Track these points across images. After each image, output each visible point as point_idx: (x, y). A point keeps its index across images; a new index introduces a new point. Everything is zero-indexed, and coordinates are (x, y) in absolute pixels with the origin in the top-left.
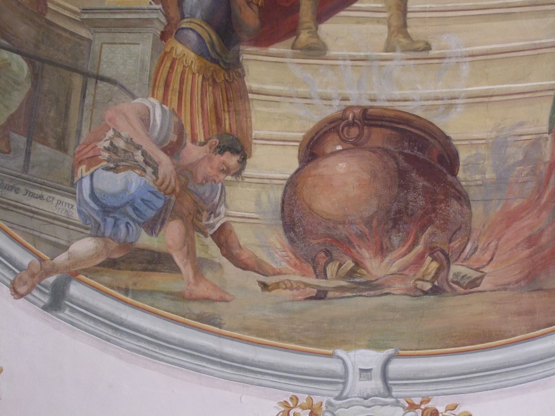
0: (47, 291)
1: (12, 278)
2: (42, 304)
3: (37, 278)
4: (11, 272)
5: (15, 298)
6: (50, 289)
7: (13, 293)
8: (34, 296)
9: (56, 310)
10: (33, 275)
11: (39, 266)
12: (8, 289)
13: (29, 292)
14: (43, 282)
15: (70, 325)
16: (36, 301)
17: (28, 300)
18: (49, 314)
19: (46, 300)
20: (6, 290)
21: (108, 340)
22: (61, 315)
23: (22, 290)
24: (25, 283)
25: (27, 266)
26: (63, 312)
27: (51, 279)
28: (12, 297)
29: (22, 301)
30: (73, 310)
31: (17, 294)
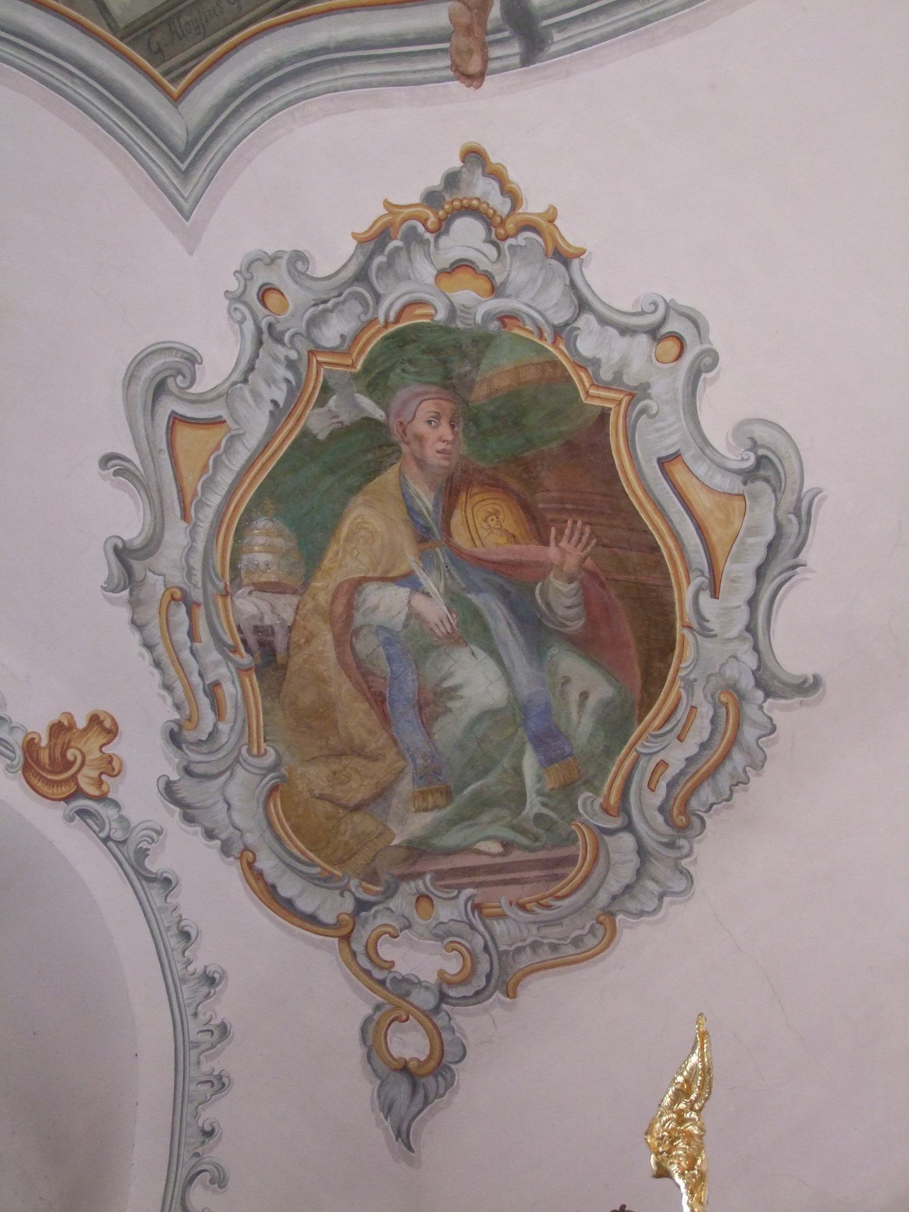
0: (506, 34)
1: (448, 62)
2: (516, 60)
3: (477, 29)
4: (439, 53)
5: (477, 87)
6: (507, 27)
7: (469, 82)
8: (497, 58)
9: (541, 50)
10: (469, 30)
11: (464, 8)
12: (457, 82)
13: (486, 60)
14: (489, 26)
15: (577, 52)
16: (505, 62)
17: (495, 72)
18: (538, 64)
19: (515, 48)
20: (457, 87)
21: (645, 22)
22: (553, 49)
23: (474, 66)
24: (470, 52)
25: (449, 23)
26: (553, 43)
27: (495, 12)
28: (472, 88)
29: (489, 82)
30: (561, 26)
31: (474, 79)
